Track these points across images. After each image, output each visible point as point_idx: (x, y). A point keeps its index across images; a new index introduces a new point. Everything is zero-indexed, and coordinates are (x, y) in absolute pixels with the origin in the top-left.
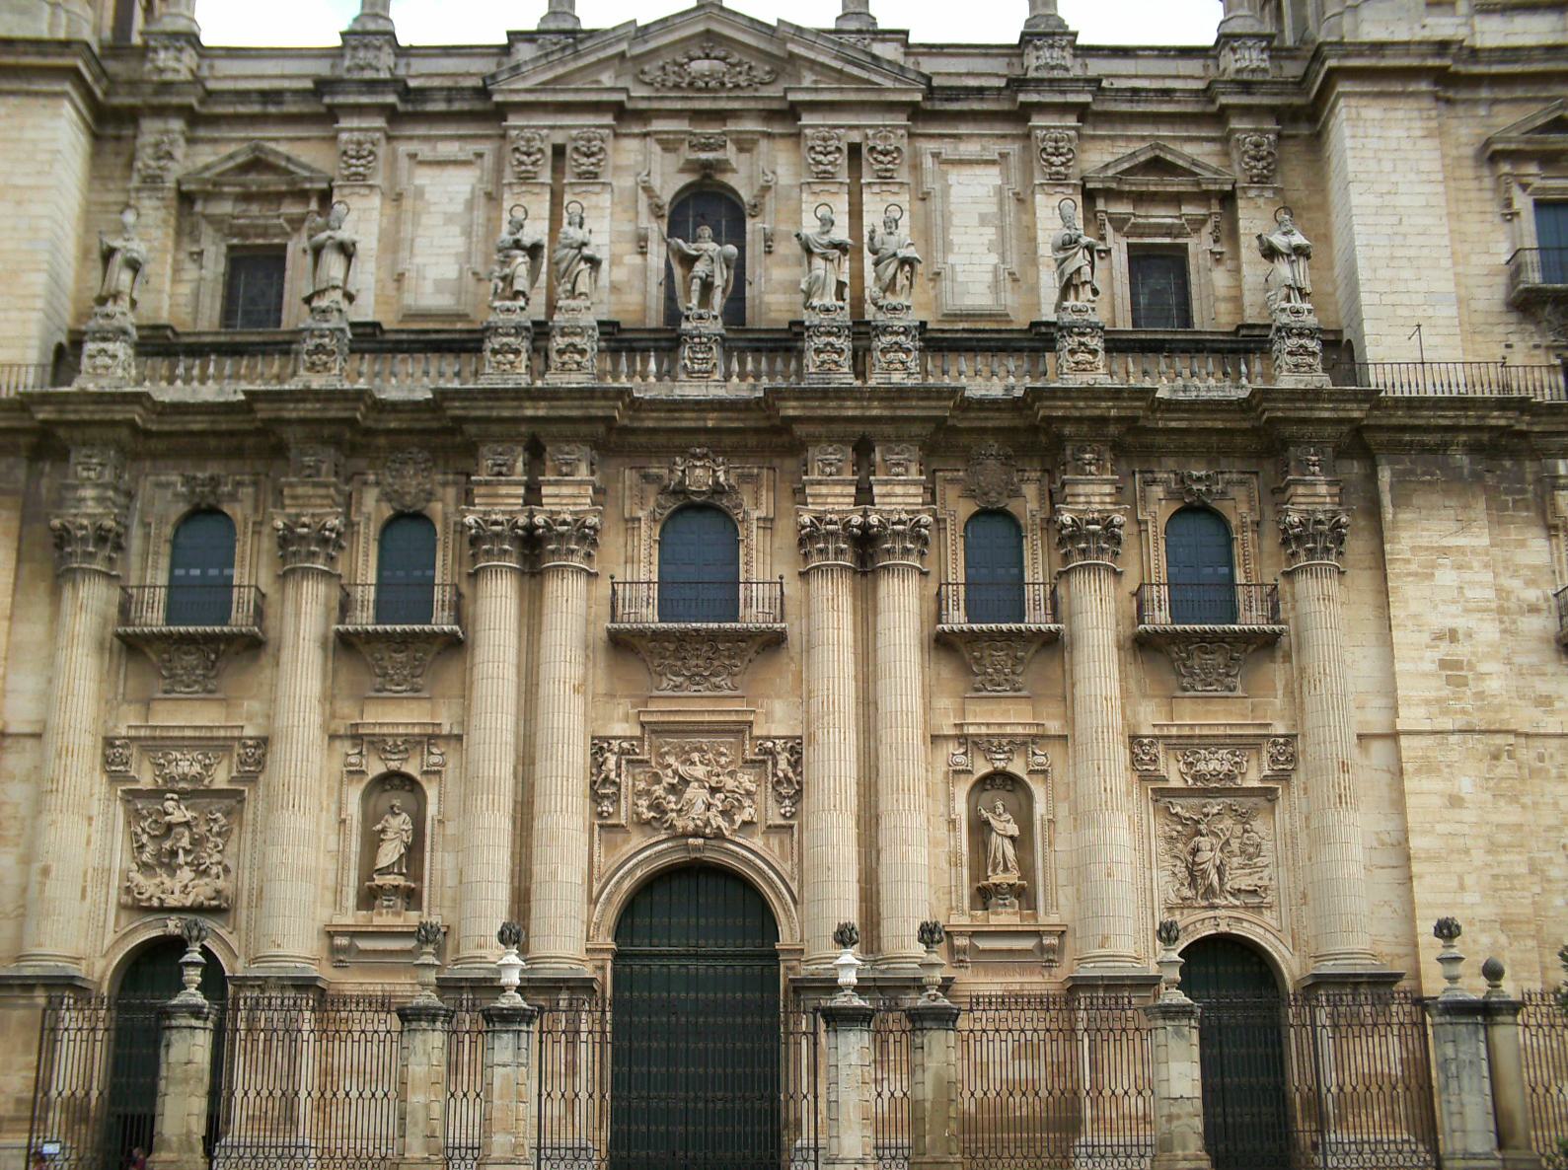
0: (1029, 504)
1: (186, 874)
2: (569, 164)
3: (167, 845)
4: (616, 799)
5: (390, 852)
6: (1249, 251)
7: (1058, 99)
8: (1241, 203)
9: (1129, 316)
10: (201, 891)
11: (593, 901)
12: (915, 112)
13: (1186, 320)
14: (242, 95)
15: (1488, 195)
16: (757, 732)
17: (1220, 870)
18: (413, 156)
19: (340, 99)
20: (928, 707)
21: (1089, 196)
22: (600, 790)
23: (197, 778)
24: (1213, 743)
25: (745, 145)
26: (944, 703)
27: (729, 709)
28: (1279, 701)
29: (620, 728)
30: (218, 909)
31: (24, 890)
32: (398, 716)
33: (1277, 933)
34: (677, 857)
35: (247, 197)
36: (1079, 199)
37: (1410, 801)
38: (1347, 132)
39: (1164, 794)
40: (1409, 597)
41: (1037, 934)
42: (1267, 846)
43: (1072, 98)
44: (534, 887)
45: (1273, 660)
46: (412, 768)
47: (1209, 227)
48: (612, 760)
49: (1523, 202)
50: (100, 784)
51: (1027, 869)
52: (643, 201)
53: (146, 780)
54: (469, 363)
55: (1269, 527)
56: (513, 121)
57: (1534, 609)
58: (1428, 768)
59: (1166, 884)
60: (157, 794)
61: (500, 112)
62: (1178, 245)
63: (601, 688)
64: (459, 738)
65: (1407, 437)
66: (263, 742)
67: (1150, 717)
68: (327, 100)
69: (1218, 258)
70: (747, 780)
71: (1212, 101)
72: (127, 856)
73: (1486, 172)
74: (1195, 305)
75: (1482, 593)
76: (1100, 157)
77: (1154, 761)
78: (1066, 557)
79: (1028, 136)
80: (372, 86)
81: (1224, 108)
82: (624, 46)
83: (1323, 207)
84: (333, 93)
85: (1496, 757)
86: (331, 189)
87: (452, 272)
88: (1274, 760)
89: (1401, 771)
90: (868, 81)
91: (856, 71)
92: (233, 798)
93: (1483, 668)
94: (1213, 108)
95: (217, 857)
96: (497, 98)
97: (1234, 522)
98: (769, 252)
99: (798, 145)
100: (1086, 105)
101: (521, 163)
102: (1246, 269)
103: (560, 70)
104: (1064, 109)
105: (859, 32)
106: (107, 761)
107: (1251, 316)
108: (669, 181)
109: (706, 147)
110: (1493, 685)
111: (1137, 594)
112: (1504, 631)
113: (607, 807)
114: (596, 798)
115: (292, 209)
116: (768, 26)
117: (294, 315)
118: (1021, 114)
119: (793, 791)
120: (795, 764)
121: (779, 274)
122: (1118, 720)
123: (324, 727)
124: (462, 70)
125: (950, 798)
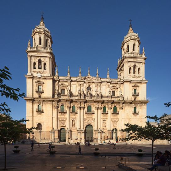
0: (106, 106)
5: (73, 124)
10: (64, 126)
14: (62, 80)
25: (91, 84)
27: (91, 117)
30: (65, 126)
32: (74, 117)
49: (133, 89)
61: (77, 82)
67: (112, 117)
70: (92, 120)
76: (111, 85)
108: (87, 86)
115: (65, 87)
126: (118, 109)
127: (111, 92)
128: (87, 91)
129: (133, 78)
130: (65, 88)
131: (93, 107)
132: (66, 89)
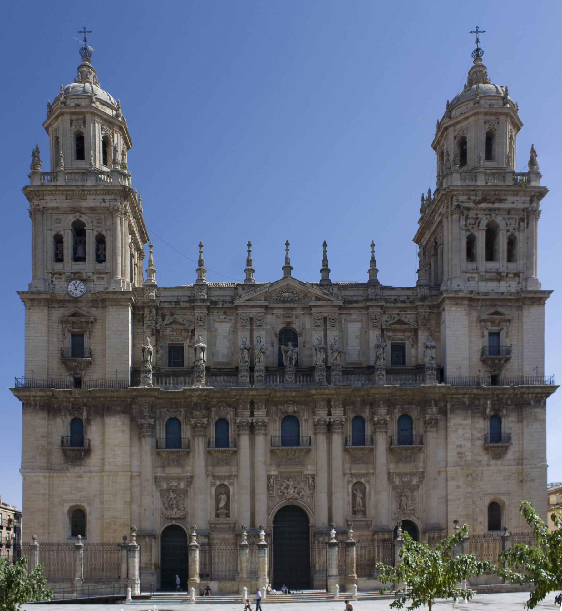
0: (366, 414)
1: (176, 509)
2: (254, 322)
3: (171, 503)
4: (273, 490)
5: (222, 504)
6: (420, 345)
7: (376, 304)
8: (419, 331)
9: (390, 362)
10: (180, 514)
11: (269, 515)
12: (340, 308)
13: (404, 363)
15: (478, 331)
16: (305, 473)
17: (406, 505)
18: (214, 320)
19: (195, 304)
20: (343, 466)
21: (382, 330)
22: (269, 488)
23: (176, 486)
24: (406, 474)
26: (347, 466)
28: (421, 464)
29: (273, 473)
31: (140, 513)
32: (222, 471)
33: (418, 518)
34: (287, 504)
35: (173, 330)
36: (380, 332)
37: (449, 487)
38: (447, 314)
39: (394, 488)
40: (452, 436)
41: (367, 521)
42: (417, 498)
43: (380, 304)
44: (256, 512)
45: (420, 453)
46: (226, 483)
47: (411, 337)
48: (272, 481)
49: (486, 333)
50: (154, 487)
51: (364, 506)
52: (272, 331)
53: (165, 486)
54: (233, 378)
55: (421, 419)
56: (240, 311)
57: (479, 439)
58: (453, 479)
59: (394, 507)
60: (168, 490)
61: (236, 308)
62: (403, 343)
63: (269, 462)
64: (237, 476)
65: (455, 396)
66: (192, 477)
68: (192, 304)
69: (413, 346)
71: (415, 303)
72: (162, 505)
73: (478, 324)
74: (406, 358)
75: (468, 436)
77: (393, 478)
78: (375, 429)
79: (368, 314)
80: (204, 301)
81: (417, 305)
82: (267, 290)
83: (439, 332)
84: (193, 302)
85: (468, 476)
86: (194, 329)
87: (226, 352)
88: (419, 478)
89: (447, 480)
90: (329, 300)
91: (326, 297)
92: (185, 492)
93: (467, 454)
94: (415, 305)
95: (182, 506)
96: (236, 304)
97: (414, 418)
98: (304, 346)
99: (311, 316)
100: (383, 305)
101: (242, 323)
102: (419, 349)
103: (251, 296)
104: (378, 306)
105: (327, 285)
106: (156, 482)
107: (420, 362)
108: (280, 326)
109: (289, 317)
110: (469, 458)
111: (391, 437)
112: (472, 445)
113: (271, 492)
114: (269, 490)
115: (184, 334)
116: (304, 283)
117: (187, 363)
118: (367, 308)
119: (313, 488)
120: (313, 481)
121: (307, 352)
122: (385, 469)
123: (206, 473)
124: (225, 294)
125: (348, 488)
126: (418, 428)
127: (389, 347)
128: (280, 349)
129: (483, 279)
130: (185, 338)
131: (306, 421)
132: (186, 344)
